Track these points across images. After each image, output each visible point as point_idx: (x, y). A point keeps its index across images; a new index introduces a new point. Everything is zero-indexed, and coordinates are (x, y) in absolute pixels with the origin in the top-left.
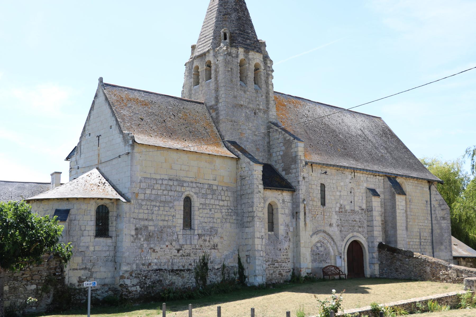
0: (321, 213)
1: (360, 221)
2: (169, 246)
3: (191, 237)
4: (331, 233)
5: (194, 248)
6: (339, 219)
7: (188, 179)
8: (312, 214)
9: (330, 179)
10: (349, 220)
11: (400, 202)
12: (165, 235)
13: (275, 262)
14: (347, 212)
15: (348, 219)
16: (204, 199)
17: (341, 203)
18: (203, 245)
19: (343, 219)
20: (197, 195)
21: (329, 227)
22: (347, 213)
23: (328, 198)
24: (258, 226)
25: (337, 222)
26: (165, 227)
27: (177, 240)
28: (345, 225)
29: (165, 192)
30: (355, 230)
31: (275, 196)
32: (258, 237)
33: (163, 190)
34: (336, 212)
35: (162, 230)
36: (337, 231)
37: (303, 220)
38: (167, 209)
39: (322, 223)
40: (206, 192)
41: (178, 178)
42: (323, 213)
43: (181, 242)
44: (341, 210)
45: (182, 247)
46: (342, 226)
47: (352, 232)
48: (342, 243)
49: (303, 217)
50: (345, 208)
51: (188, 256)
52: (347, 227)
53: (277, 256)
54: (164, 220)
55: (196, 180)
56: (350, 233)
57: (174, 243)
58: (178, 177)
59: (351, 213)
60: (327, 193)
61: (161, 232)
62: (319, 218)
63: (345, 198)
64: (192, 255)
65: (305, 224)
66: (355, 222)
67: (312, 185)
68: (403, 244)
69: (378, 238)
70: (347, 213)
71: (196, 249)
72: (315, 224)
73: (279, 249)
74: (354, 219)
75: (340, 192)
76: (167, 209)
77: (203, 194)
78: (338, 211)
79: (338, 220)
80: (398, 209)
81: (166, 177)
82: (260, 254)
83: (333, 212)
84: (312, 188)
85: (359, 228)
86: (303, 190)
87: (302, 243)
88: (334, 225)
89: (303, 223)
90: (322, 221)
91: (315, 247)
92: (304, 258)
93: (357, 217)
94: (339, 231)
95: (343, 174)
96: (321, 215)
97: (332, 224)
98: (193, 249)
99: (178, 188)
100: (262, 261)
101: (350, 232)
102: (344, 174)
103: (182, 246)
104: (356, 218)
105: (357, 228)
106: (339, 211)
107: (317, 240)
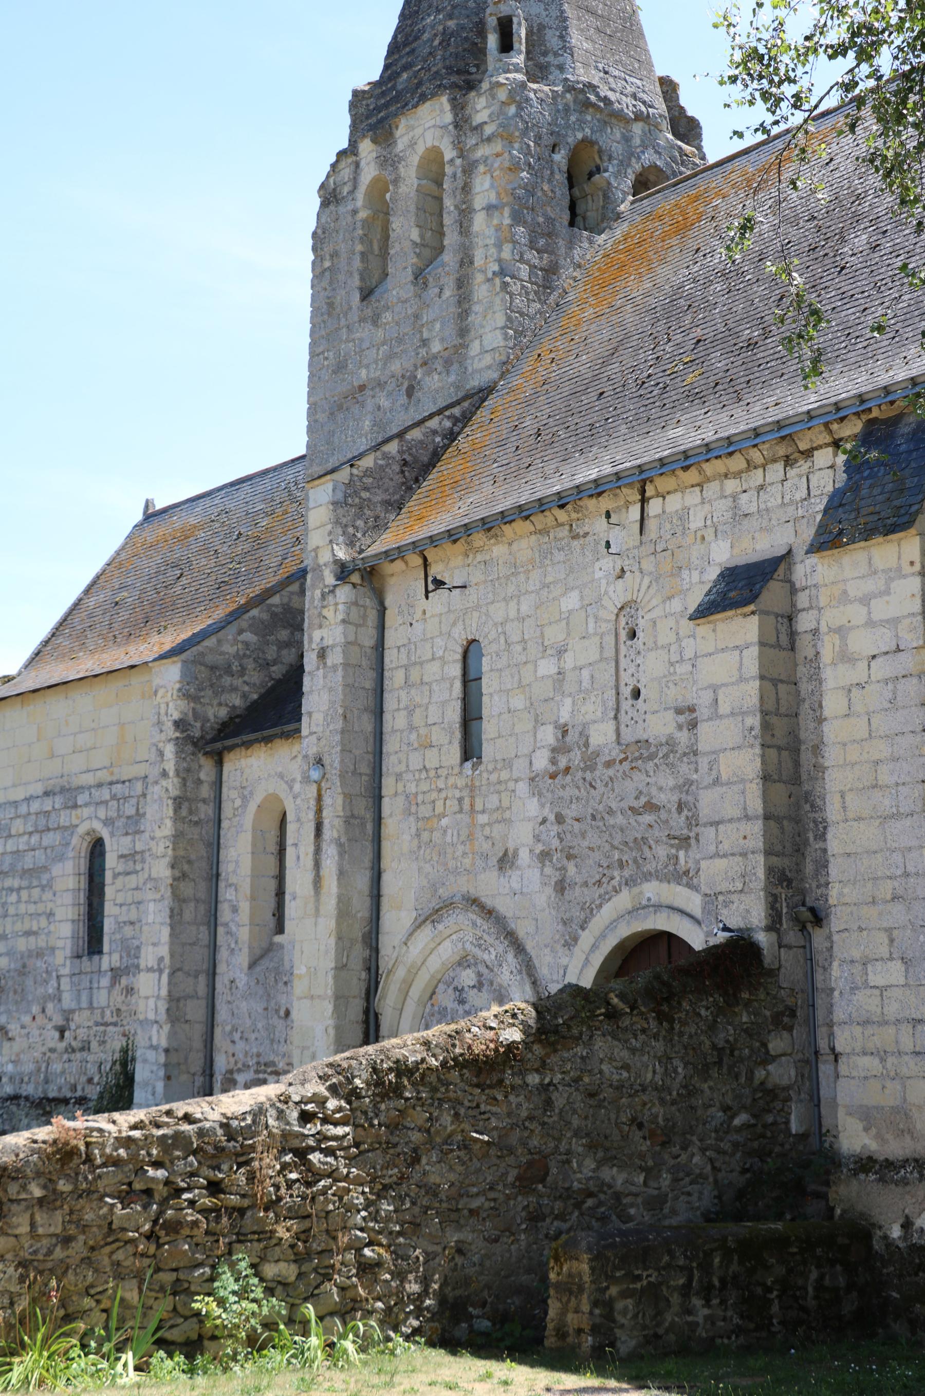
0: (460, 800)
1: (680, 807)
2: (40, 1019)
3: (91, 982)
4: (504, 906)
5: (100, 1020)
6: (552, 817)
7: (88, 779)
9: (504, 600)
10: (611, 812)
11: (865, 600)
12: (29, 982)
13: (269, 1070)
14: (600, 767)
15: (601, 808)
16: (129, 838)
17: (565, 716)
18: (124, 1008)
19: (570, 813)
20: (110, 828)
21: (496, 873)
23: (495, 711)
24: (150, 920)
25: (537, 837)
26: (30, 954)
27: (57, 997)
28: (586, 844)
29: (34, 839)
30: (650, 867)
31: (280, 769)
32: (150, 966)
33: (31, 833)
34: (532, 779)
35: (24, 966)
37: (309, 862)
38: (36, 892)
39: (465, 854)
40: (138, 809)
41: (64, 782)
42: (467, 801)
43: (68, 1001)
44: (563, 762)
45: (68, 1020)
46: (569, 857)
47: (629, 882)
48: (564, 961)
49: (311, 849)
50: (587, 745)
51: (82, 1049)
52: (597, 856)
53: (275, 1046)
54: (28, 933)
55: (112, 774)
56: (617, 891)
57: (50, 1006)
58: (65, 778)
59: (621, 762)
60: (489, 684)
61: (23, 971)
62: (449, 831)
63: (586, 684)
64: (94, 1045)
65: (317, 881)
66: (648, 818)
67: (421, 664)
68: (889, 930)
69: (726, 904)
70: (597, 773)
71: (106, 1024)
72: (428, 868)
73: (282, 1013)
74: (643, 800)
75: (561, 652)
76: (36, 892)
77: (128, 818)
78: (546, 770)
79: (544, 821)
80: (845, 657)
81: (38, 789)
82: (150, 1039)
83: (516, 781)
85: (679, 848)
86: (315, 716)
87: (300, 977)
88: (524, 856)
89: (310, 876)
90: (461, 848)
91: (450, 991)
92: (304, 1048)
93: (662, 782)
94: (549, 890)
95: (575, 543)
96: (461, 811)
97: (510, 853)
98: (97, 1024)
99: (64, 818)
100: (155, 1068)
101: (615, 882)
102: (586, 534)
103: (68, 1015)
104: (654, 790)
105: (662, 852)
106: (552, 769)
107: (447, 951)
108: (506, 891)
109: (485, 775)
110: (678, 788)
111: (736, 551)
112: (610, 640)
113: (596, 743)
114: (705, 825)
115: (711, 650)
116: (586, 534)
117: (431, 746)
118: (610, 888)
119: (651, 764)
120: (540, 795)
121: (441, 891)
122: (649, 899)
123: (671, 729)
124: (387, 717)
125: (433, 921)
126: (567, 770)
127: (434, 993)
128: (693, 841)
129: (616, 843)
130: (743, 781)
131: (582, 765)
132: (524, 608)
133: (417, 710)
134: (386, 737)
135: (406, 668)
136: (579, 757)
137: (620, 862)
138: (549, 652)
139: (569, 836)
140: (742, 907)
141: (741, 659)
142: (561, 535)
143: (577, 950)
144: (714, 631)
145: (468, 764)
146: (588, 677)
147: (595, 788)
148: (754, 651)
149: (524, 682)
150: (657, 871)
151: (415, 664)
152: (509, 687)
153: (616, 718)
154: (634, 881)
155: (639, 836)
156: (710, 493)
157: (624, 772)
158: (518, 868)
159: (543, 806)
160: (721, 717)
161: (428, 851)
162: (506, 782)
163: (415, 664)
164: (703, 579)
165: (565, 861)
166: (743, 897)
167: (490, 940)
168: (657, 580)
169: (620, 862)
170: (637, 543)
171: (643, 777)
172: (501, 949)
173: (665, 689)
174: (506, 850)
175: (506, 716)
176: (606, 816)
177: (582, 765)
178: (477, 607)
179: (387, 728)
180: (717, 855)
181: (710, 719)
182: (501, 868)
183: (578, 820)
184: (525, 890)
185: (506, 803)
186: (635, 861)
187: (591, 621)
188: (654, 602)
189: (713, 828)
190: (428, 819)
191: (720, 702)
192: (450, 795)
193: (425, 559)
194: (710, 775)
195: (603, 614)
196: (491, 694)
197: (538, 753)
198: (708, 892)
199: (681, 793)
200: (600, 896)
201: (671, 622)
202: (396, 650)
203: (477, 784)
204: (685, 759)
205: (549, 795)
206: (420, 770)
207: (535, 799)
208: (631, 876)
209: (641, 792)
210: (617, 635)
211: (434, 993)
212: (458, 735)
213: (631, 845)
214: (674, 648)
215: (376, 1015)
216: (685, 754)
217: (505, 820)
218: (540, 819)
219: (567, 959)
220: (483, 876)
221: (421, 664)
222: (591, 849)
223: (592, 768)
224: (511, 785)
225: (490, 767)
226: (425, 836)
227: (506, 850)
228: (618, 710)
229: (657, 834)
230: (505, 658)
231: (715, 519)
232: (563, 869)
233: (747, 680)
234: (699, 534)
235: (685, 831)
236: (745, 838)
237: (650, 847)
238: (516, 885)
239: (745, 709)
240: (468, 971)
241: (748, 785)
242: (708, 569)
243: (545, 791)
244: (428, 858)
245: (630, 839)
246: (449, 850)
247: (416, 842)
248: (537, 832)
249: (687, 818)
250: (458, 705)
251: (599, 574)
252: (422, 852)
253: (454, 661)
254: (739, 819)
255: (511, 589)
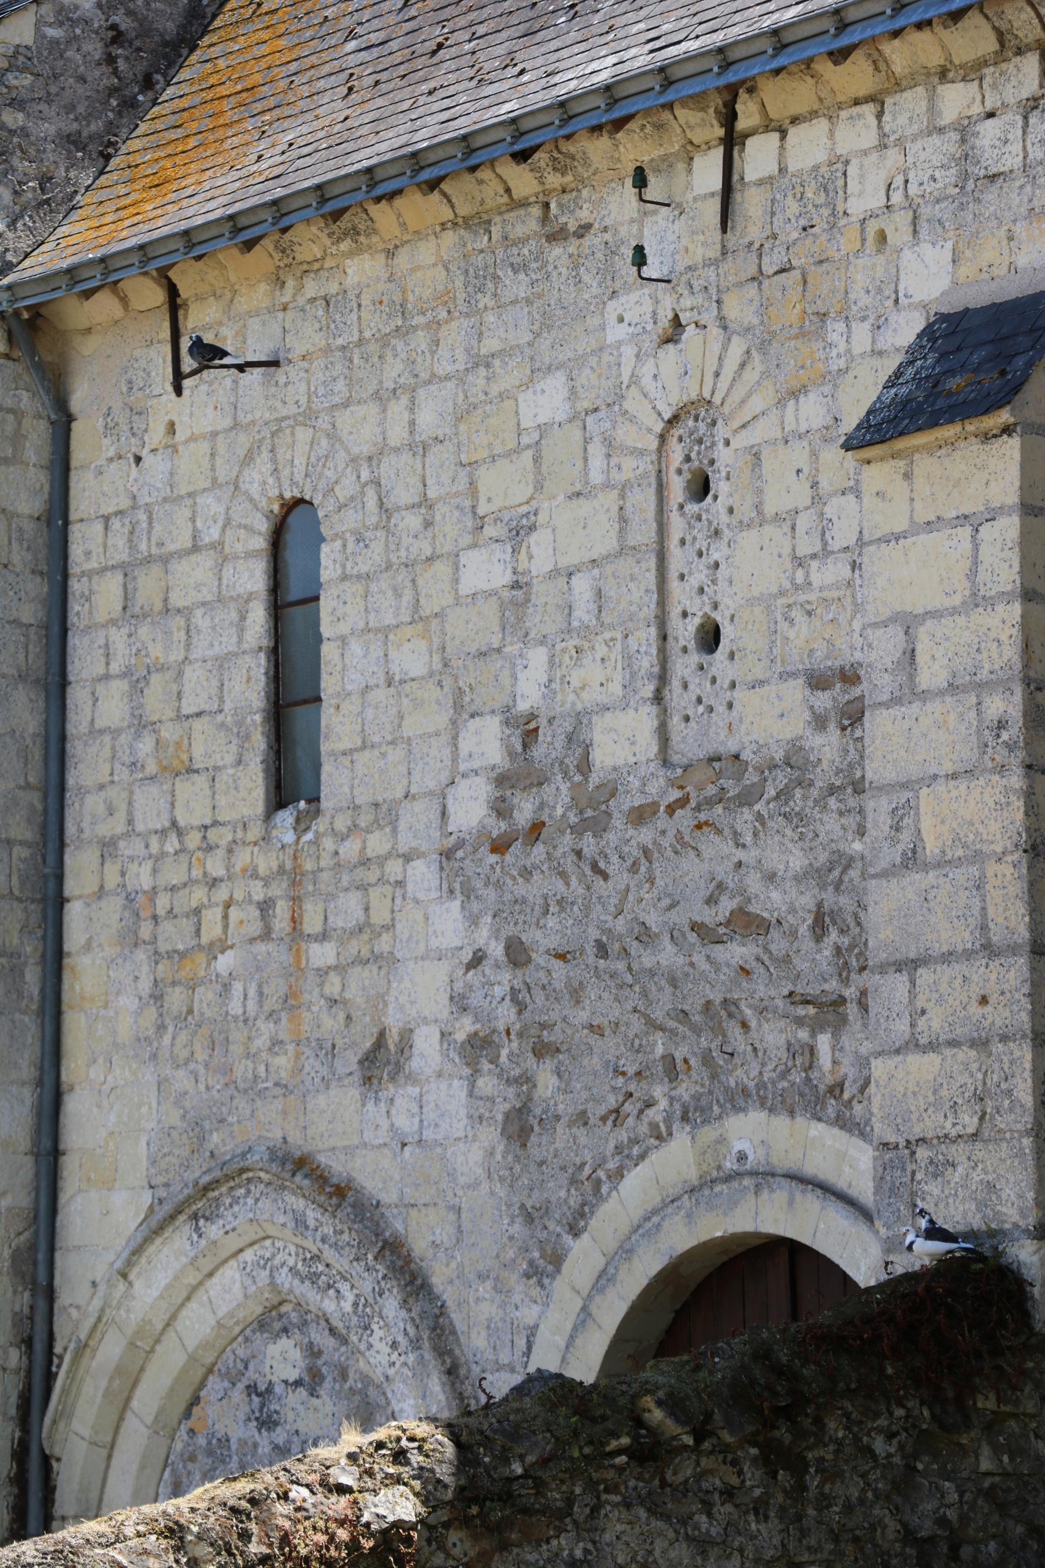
0: (265, 907)
6: (497, 950)
8: (157, 956)
9: (376, 396)
10: (645, 936)
15: (620, 925)
21: (354, 1093)
22: (619, 830)
23: (355, 681)
25: (460, 1003)
28: (583, 1016)
34: (447, 854)
36: (459, 1126)
39: (276, 1043)
42: (282, 910)
44: (525, 812)
46: (542, 1050)
48: (529, 1314)
50: (585, 766)
52: (610, 1046)
56: (661, 1137)
59: (671, 810)
62: (238, 987)
63: (583, 613)
67: (165, 560)
69: (938, 1169)
72: (182, 1080)
74: (727, 905)
79: (477, 960)
84: (177, 600)
90: (266, 1029)
93: (774, 860)
94: (490, 1135)
95: (556, 252)
96: (267, 934)
101: (656, 1114)
102: (585, 228)
104: (754, 883)
106: (498, 828)
108: (383, 1137)
109: (328, 844)
110: (816, 875)
111: (966, 271)
112: (644, 500)
113: (609, 762)
114: (882, 969)
115: (900, 525)
116: (585, 228)
117: (191, 771)
118: (644, 1129)
119: (747, 814)
120: (468, 893)
121: (215, 1138)
122: (742, 1157)
123: (796, 726)
124: (78, 696)
125: (195, 1217)
126: (536, 829)
127: (195, 1400)
128: (852, 1010)
129: (658, 1014)
130: (978, 857)
131: (573, 819)
132: (428, 420)
133: (155, 679)
134: (75, 748)
135: (126, 570)
136: (565, 797)
137: (669, 1060)
138: (490, 531)
139: (539, 997)
140: (977, 1176)
141: (976, 548)
142: (519, 231)
143: (560, 1286)
144: (907, 476)
145: (286, 817)
146: (588, 595)
147: (605, 876)
148: (1009, 527)
149: (428, 608)
150: (761, 1085)
151: (149, 560)
152: (389, 619)
153: (658, 698)
154: (704, 1110)
155: (717, 997)
156: (902, 120)
157: (679, 836)
158: (412, 1079)
159: (473, 921)
160: (924, 696)
161: (183, 1037)
162: (382, 860)
163: (149, 560)
164: (880, 345)
165: (531, 1061)
166: (979, 1151)
167: (340, 1262)
168: (763, 347)
169: (669, 1060)
170: (714, 252)
171: (727, 847)
172: (367, 1286)
173: (783, 626)
174: (382, 1034)
175: (380, 695)
176: (634, 947)
177: (573, 819)
178: (308, 417)
179: (77, 723)
180: (913, 1045)
181: (895, 701)
182: (367, 1080)
183: (562, 957)
184: (428, 1134)
185: (380, 916)
186: (707, 1059)
187: (596, 450)
188: (756, 404)
189: (904, 977)
190: (183, 955)
191: (921, 658)
192: (239, 896)
193: (173, 292)
194: (894, 841)
195: (626, 435)
196: (343, 640)
197: (463, 787)
198: (892, 1138)
199: (823, 887)
200: (618, 1149)
201: (798, 455)
202: (99, 527)
203: (309, 866)
204: (833, 803)
205: (490, 894)
206: (163, 833)
207: (456, 905)
208: (696, 1098)
209: (721, 886)
210: (661, 488)
211: (195, 1400)
212: (259, 742)
213: (697, 1018)
214: (804, 522)
215: (46, 1462)
216: (832, 790)
217: (377, 958)
218: (467, 956)
219: (536, 1309)
220: (322, 1100)
221: (165, 560)
222: (596, 1029)
223: (598, 826)
224: (394, 868)
225: (342, 823)
226: (176, 998)
227: (382, 1034)
228: (663, 678)
229: (761, 991)
230: (377, 548)
231: (913, 189)
232: (527, 1079)
233: (990, 602)
234: (872, 227)
235: (833, 985)
236: (984, 1000)
237: (745, 1025)
238: (406, 1123)
239: (984, 675)
240: (285, 1343)
241: (992, 868)
242: (893, 317)
243: (478, 884)
244: (185, 1053)
245: (694, 1005)
246: (237, 1035)
247: (152, 1013)
248: (459, 986)
249: (838, 950)
250: (258, 667)
251: (616, 333)
252: (167, 1040)
253: (249, 555)
254: (969, 955)
255: (393, 370)
